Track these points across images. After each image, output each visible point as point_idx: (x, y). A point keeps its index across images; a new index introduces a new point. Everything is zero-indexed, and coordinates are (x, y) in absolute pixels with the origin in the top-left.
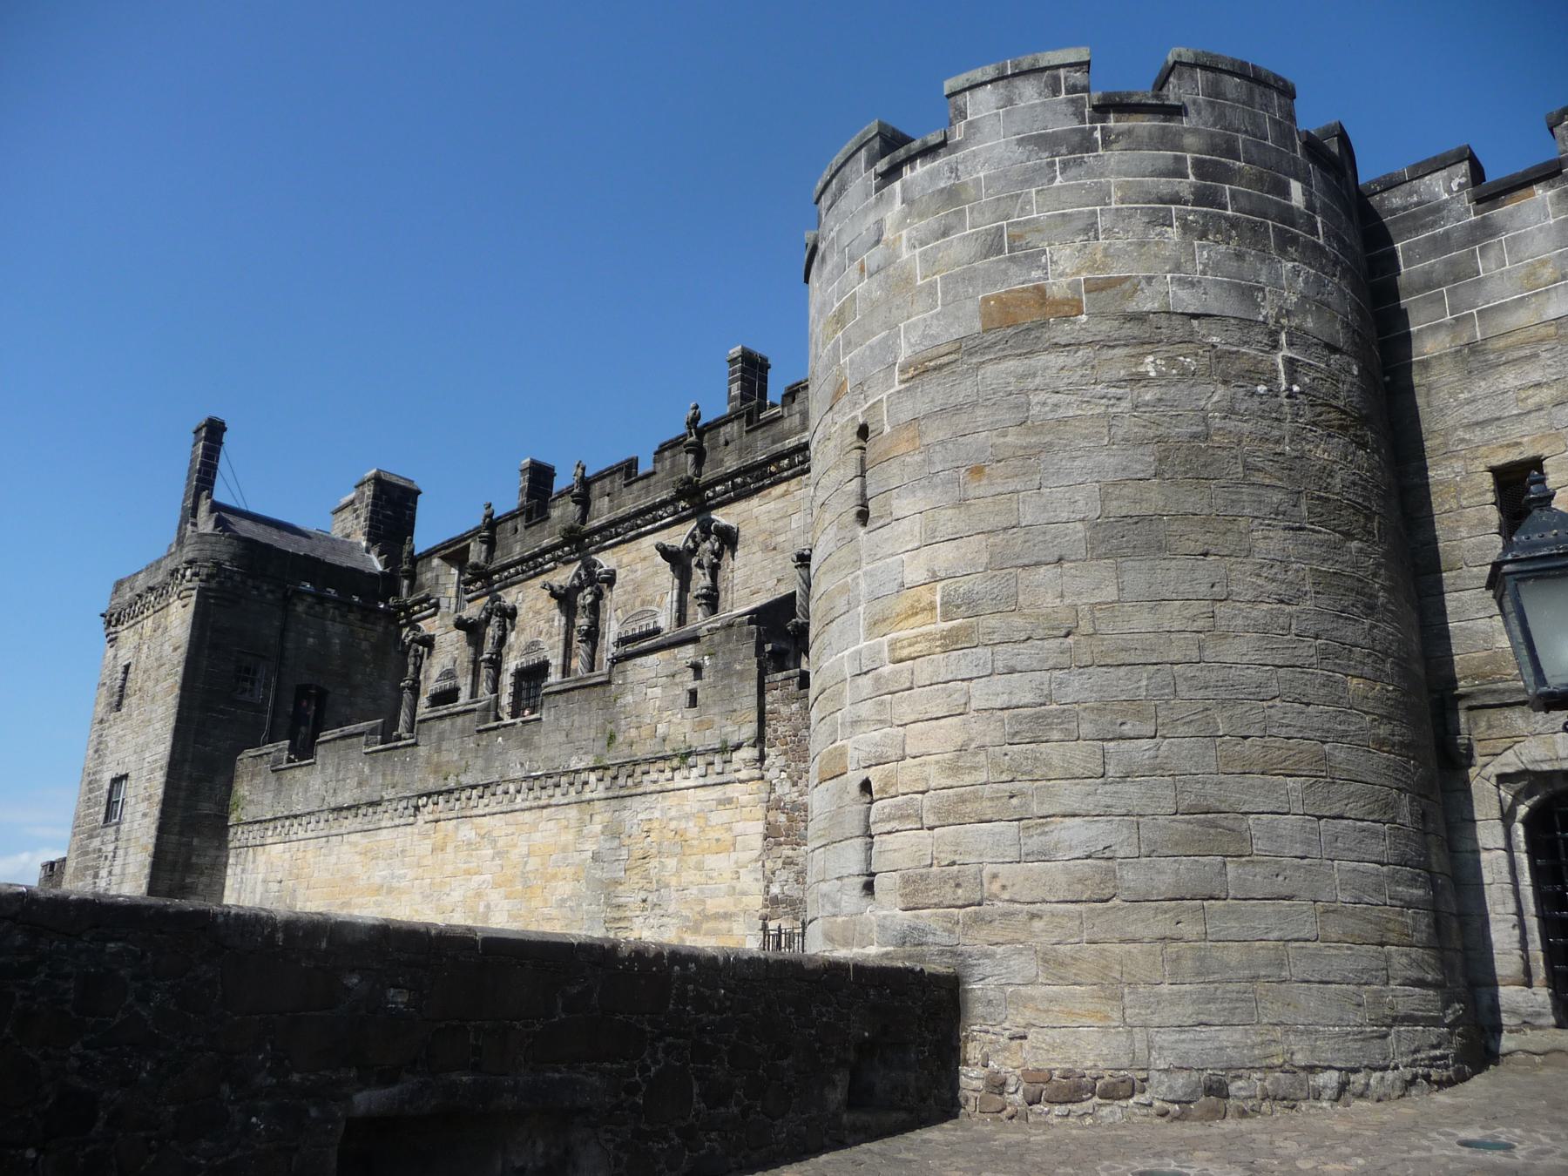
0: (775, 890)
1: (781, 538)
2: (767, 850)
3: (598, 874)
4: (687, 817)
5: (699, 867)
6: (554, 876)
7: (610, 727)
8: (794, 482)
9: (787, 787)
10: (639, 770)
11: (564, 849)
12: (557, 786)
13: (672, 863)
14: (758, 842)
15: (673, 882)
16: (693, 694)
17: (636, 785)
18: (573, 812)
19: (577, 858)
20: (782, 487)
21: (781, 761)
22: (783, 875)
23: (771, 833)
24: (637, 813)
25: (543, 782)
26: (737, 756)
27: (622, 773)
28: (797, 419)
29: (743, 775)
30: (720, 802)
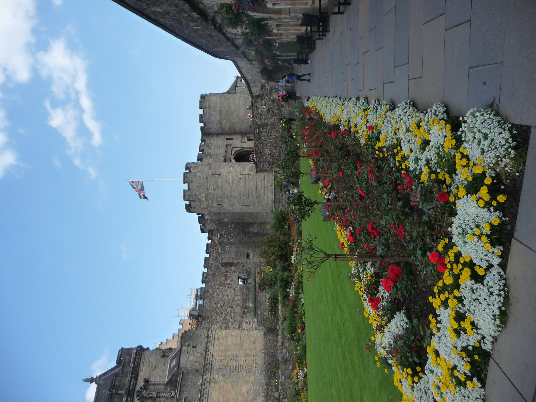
0: (237, 327)
1: (154, 364)
2: (229, 329)
3: (228, 375)
4: (219, 349)
5: (230, 346)
6: (226, 391)
7: (194, 371)
8: (142, 360)
9: (218, 324)
10: (207, 362)
11: (220, 387)
12: (204, 390)
13: (228, 353)
14: (228, 331)
15: (232, 352)
16: (194, 347)
17: (209, 363)
18: (212, 385)
19: (223, 382)
20: (141, 364)
21: (213, 326)
22: (234, 324)
23: (226, 328)
24: (216, 364)
25: (202, 394)
26: (209, 336)
27: (206, 367)
28: (128, 357)
29: (214, 334)
30: (218, 340)
